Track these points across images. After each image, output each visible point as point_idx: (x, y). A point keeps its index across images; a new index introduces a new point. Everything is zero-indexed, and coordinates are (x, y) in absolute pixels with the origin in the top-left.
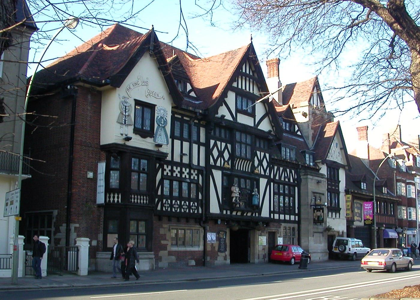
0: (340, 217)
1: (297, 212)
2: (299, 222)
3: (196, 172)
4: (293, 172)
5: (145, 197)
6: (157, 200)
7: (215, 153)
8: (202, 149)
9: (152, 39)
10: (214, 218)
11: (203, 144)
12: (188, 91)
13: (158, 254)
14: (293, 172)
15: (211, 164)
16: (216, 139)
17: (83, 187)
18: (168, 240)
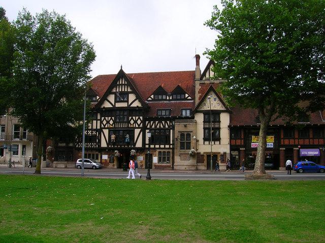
1: (171, 143)
2: (173, 149)
4: (168, 122)
7: (105, 122)
8: (99, 122)
10: (104, 149)
11: (99, 120)
14: (168, 122)
16: (105, 117)
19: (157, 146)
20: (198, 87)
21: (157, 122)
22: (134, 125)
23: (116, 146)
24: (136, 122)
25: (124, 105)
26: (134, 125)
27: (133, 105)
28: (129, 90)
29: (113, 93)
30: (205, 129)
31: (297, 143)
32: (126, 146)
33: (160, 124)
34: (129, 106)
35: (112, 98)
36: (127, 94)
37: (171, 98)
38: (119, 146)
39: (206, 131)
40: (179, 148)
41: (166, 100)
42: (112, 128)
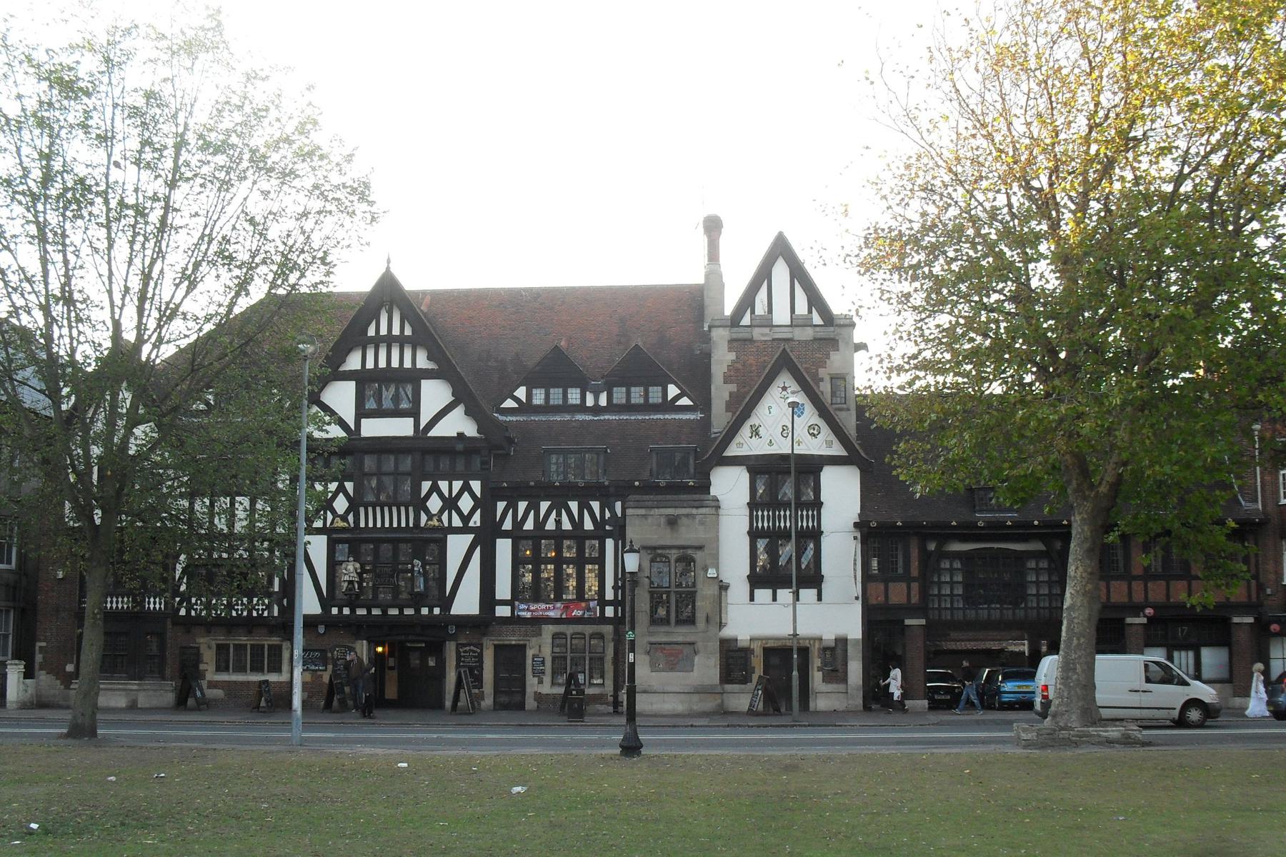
0: (820, 598)
4: (596, 505)
14: (596, 505)
17: (53, 591)
20: (722, 358)
21: (544, 506)
22: (445, 517)
23: (361, 612)
24: (450, 504)
25: (401, 427)
26: (445, 517)
28: (423, 362)
30: (754, 534)
31: (1138, 597)
32: (409, 612)
33: (559, 514)
34: (421, 433)
35: (342, 397)
36: (414, 377)
37: (603, 401)
38: (376, 612)
39: (761, 544)
40: (642, 619)
42: (343, 530)
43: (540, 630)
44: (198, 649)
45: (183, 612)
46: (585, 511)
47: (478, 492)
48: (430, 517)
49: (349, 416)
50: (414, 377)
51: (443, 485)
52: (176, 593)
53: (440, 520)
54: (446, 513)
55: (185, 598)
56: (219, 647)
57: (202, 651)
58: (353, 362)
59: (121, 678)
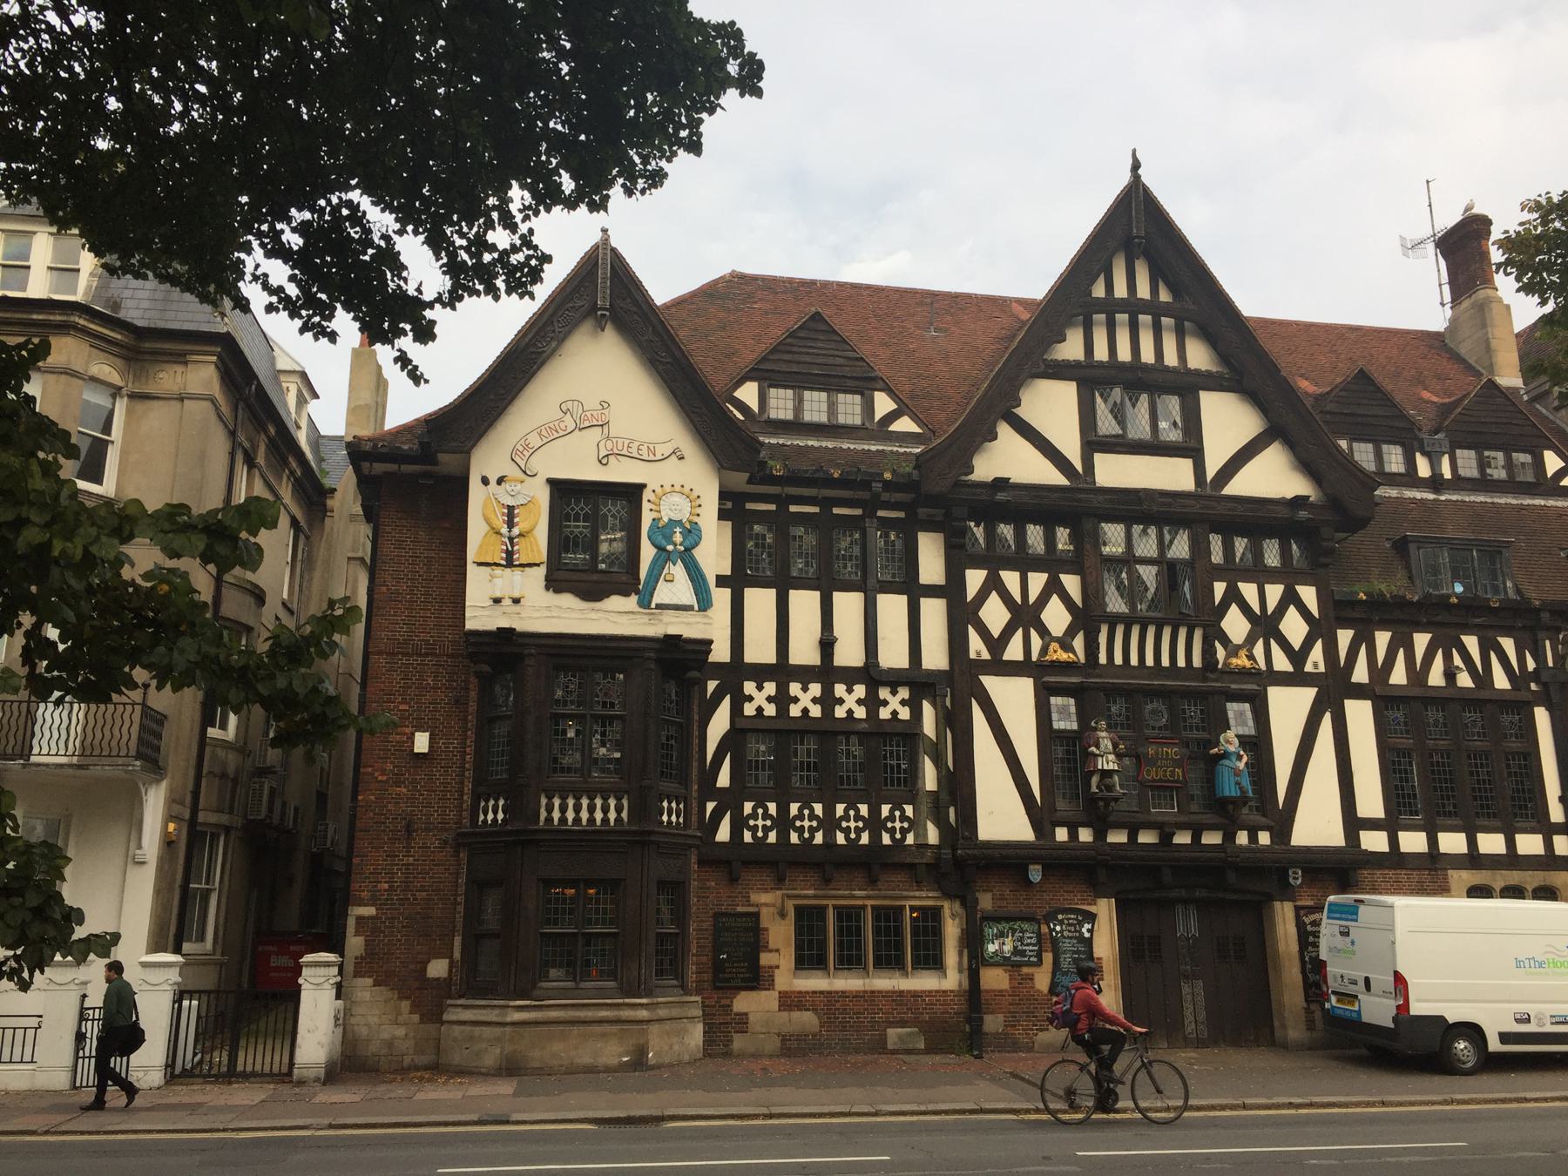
3: (904, 693)
4: (1508, 644)
5: (674, 805)
6: (710, 806)
7: (995, 614)
8: (934, 612)
9: (604, 272)
11: (933, 591)
12: (877, 418)
13: (730, 1006)
14: (1508, 644)
15: (973, 655)
16: (994, 561)
17: (398, 784)
18: (777, 951)
19: (1453, 842)
21: (1421, 641)
22: (1259, 650)
23: (1118, 837)
24: (1265, 626)
25: (1174, 475)
26: (1259, 650)
27: (1246, 484)
29: (1060, 371)
32: (1212, 838)
33: (1448, 658)
36: (1187, 386)
38: (1147, 838)
41: (1409, 478)
43: (1446, 877)
44: (756, 916)
45: (723, 834)
46: (1492, 654)
47: (1313, 607)
48: (1233, 650)
49: (1070, 444)
50: (1187, 386)
51: (1249, 591)
52: (709, 789)
53: (1251, 657)
54: (1260, 644)
55: (730, 801)
56: (799, 910)
57: (764, 923)
58: (1071, 348)
59: (602, 993)
